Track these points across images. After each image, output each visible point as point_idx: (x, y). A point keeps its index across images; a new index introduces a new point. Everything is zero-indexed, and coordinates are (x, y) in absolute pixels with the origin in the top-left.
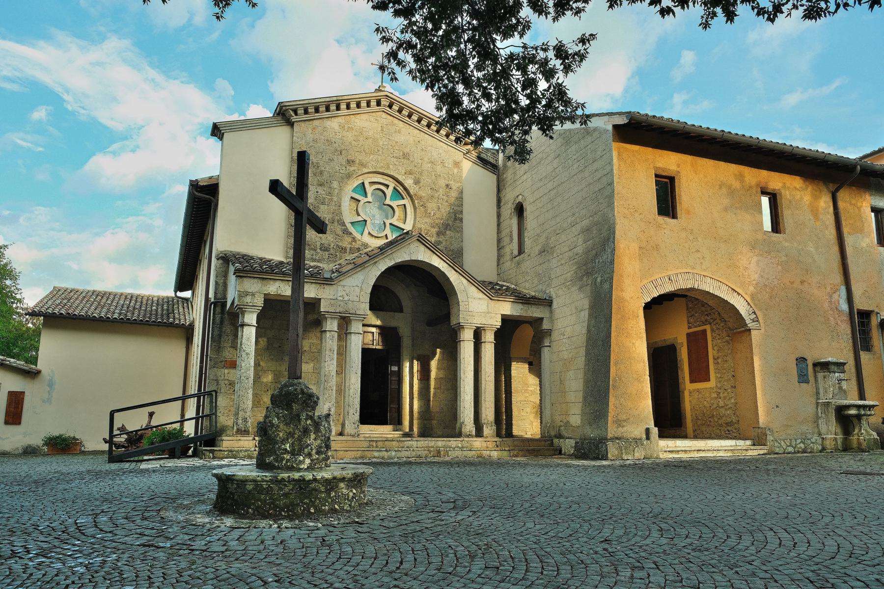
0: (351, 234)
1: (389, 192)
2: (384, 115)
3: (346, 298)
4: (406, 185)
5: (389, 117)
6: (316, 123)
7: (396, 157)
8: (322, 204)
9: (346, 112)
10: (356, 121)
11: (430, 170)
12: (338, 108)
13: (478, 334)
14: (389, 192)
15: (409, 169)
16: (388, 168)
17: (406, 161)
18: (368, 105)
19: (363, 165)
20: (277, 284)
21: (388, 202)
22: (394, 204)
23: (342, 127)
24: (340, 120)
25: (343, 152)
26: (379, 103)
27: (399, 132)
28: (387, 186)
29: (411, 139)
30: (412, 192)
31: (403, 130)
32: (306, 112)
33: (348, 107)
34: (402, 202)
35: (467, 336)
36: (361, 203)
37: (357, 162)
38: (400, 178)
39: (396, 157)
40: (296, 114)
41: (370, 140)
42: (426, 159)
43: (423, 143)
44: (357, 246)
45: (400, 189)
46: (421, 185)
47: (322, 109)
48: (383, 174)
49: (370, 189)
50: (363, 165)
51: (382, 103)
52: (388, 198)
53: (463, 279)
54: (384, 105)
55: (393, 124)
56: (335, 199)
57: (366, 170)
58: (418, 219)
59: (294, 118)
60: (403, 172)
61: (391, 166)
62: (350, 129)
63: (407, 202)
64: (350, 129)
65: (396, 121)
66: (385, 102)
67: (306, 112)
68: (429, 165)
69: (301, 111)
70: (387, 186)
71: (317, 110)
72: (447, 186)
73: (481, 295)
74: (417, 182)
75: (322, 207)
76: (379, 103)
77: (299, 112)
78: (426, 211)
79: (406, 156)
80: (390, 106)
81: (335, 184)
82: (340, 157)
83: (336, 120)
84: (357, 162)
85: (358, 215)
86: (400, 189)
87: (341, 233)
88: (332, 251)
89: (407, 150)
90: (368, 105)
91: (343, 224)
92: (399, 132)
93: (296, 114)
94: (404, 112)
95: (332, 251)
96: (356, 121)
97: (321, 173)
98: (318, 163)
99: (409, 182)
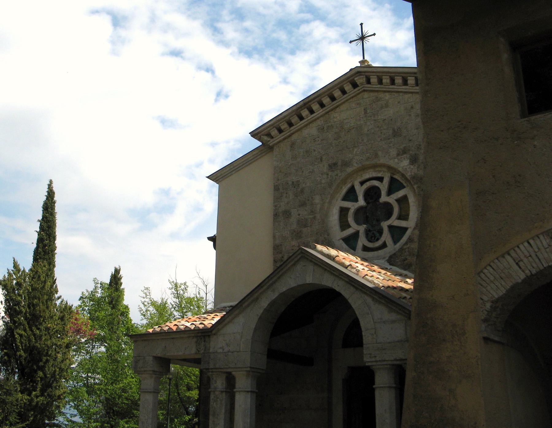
1: (384, 187)
2: (366, 95)
3: (226, 350)
5: (372, 94)
6: (294, 137)
8: (305, 226)
12: (312, 112)
13: (399, 372)
16: (376, 155)
21: (384, 198)
23: (321, 129)
24: (319, 122)
25: (324, 158)
26: (355, 85)
27: (387, 106)
28: (381, 179)
30: (408, 175)
32: (280, 131)
34: (400, 194)
35: (383, 380)
36: (351, 212)
37: (340, 163)
40: (272, 138)
45: (396, 177)
47: (295, 119)
49: (360, 191)
50: (346, 164)
52: (384, 193)
53: (366, 297)
54: (362, 84)
56: (318, 216)
57: (349, 170)
59: (271, 142)
61: (380, 153)
65: (381, 95)
67: (280, 131)
69: (274, 132)
70: (381, 179)
73: (394, 316)
74: (414, 160)
75: (305, 230)
76: (355, 85)
79: (396, 133)
80: (368, 81)
83: (314, 124)
84: (340, 163)
85: (349, 226)
93: (272, 138)
94: (384, 81)
97: (302, 191)
98: (298, 181)
99: (404, 164)
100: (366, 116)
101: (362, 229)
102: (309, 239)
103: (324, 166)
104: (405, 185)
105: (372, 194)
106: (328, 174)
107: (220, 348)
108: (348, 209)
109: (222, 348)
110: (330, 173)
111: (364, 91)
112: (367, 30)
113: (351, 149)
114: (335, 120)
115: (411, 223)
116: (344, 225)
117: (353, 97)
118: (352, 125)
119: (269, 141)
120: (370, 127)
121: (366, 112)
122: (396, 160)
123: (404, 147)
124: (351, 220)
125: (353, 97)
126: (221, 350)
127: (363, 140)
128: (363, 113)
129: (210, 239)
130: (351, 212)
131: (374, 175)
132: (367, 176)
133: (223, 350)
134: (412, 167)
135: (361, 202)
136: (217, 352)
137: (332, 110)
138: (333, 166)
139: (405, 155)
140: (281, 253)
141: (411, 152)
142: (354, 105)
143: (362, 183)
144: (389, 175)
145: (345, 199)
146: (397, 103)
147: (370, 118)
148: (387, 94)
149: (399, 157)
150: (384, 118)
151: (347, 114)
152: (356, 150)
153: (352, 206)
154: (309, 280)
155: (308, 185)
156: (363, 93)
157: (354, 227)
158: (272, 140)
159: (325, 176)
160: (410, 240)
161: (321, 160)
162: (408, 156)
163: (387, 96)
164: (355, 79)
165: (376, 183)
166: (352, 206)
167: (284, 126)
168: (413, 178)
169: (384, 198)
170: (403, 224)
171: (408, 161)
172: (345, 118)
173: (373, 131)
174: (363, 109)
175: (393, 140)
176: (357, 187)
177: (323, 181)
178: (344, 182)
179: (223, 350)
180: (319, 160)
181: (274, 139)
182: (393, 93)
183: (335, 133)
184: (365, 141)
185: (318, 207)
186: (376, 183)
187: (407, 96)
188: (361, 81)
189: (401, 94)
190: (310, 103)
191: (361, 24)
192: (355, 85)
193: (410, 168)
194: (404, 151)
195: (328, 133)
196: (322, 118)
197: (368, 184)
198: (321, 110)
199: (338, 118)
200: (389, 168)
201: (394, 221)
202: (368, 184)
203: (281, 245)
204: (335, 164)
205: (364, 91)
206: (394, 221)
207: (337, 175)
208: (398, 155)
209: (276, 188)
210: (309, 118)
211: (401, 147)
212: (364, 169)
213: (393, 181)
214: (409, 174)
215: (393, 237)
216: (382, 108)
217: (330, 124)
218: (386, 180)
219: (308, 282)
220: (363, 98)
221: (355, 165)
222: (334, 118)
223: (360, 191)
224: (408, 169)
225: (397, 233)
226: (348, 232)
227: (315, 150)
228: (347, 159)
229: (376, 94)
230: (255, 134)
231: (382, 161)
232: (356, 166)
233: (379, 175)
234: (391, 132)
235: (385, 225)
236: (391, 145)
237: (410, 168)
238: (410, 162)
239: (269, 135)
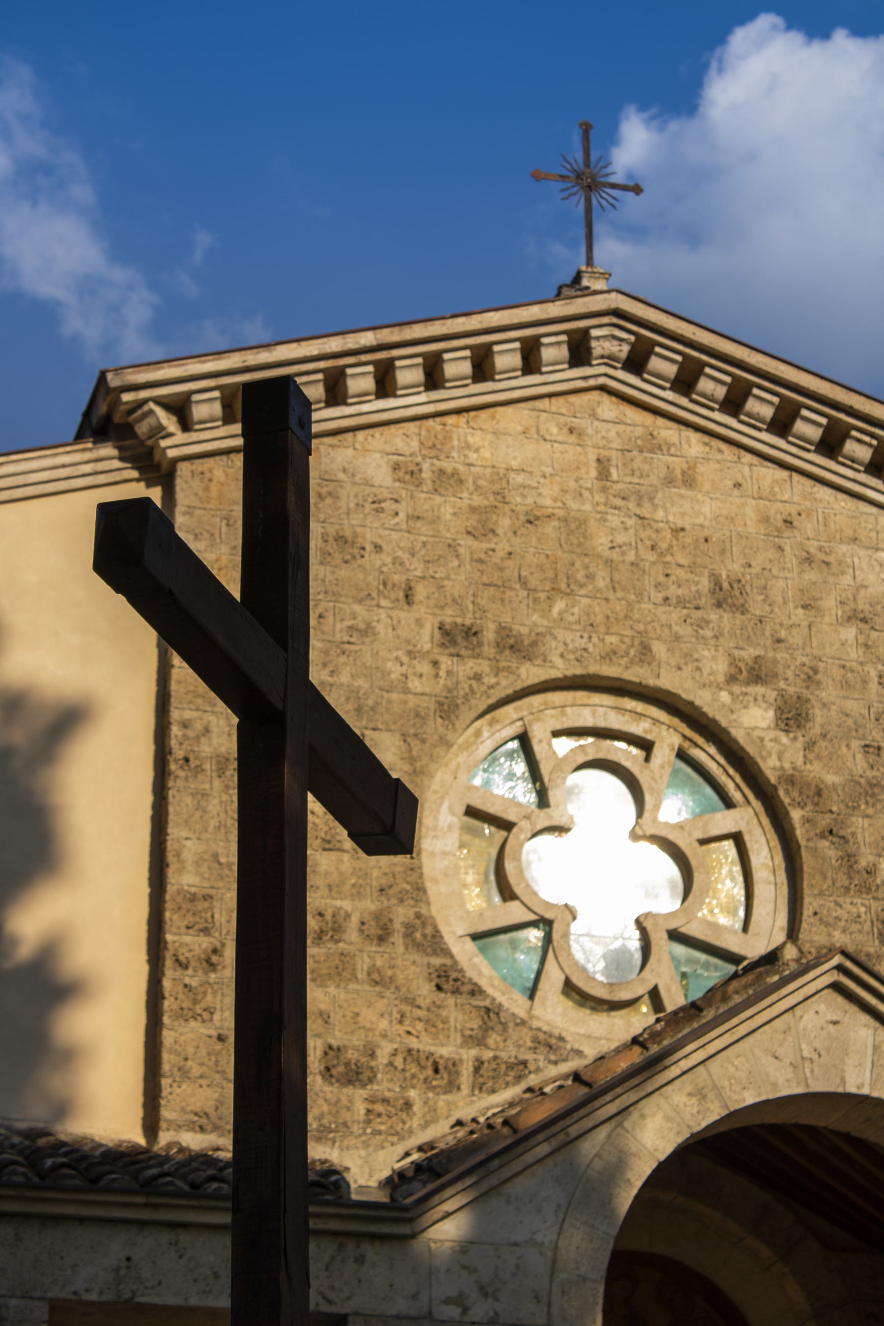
0: (476, 991)
2: (608, 408)
4: (738, 734)
7: (681, 602)
9: (421, 401)
10: (475, 439)
11: (854, 654)
12: (385, 385)
15: (749, 653)
16: (645, 653)
17: (725, 620)
18: (531, 361)
19: (515, 647)
20: (115, 1246)
23: (407, 472)
25: (421, 591)
27: (689, 480)
29: (750, 511)
30: (770, 767)
31: (706, 471)
33: (433, 378)
37: (490, 634)
38: (713, 703)
39: (681, 602)
40: (186, 425)
41: (550, 528)
42: (830, 603)
43: (808, 527)
44: (509, 1053)
46: (816, 730)
51: (598, 348)
54: (609, 359)
55: (653, 445)
58: (810, 904)
60: (722, 667)
61: (659, 649)
62: (447, 480)
63: (747, 818)
64: (447, 480)
65: (668, 432)
66: (607, 343)
68: (850, 633)
74: (792, 716)
76: (579, 352)
77: (199, 412)
78: (849, 859)
79: (726, 595)
80: (636, 363)
82: (405, 616)
83: (377, 439)
84: (490, 634)
86: (708, 755)
87: (425, 990)
88: (384, 1086)
89: (731, 567)
90: (531, 361)
91: (435, 943)
92: (689, 480)
94: (704, 385)
95: (385, 1085)
96: (475, 439)
99: (751, 720)
100: (604, 490)
102: (346, 905)
103: (419, 622)
104: (736, 796)
106: (435, 663)
107: (448, 1301)
109: (459, 1300)
110: (446, 663)
111: (603, 388)
113: (542, 596)
114: (473, 457)
117: (550, 395)
118: (548, 502)
119: (170, 435)
120: (621, 538)
121: (604, 474)
122: (724, 696)
123: (757, 658)
125: (550, 395)
126: (453, 1312)
127: (590, 577)
128: (593, 473)
131: (615, 722)
133: (465, 1310)
134: (784, 739)
136: (430, 1315)
137: (458, 412)
138: (457, 637)
139: (759, 689)
140: (206, 931)
141: (782, 684)
142: (554, 430)
144: (676, 740)
146: (730, 484)
147: (618, 502)
148: (695, 437)
149: (737, 689)
150: (680, 524)
152: (559, 605)
155: (344, 678)
156: (595, 395)
158: (180, 437)
159: (425, 668)
161: (408, 598)
162: (772, 695)
163: (694, 445)
164: (594, 333)
168: (791, 780)
171: (771, 714)
172: (514, 464)
173: (631, 556)
174: (592, 457)
175: (713, 616)
177: (415, 684)
179: (465, 1310)
180: (401, 595)
181: (194, 436)
182: (716, 443)
183: (473, 509)
184: (601, 583)
187: (772, 473)
188: (611, 347)
189: (748, 457)
190: (395, 353)
192: (579, 352)
193: (775, 740)
194: (757, 674)
195: (438, 499)
196: (411, 427)
198: (423, 398)
199: (486, 453)
203: (207, 897)
204: (471, 633)
205: (603, 388)
207: (478, 677)
208: (732, 679)
210: (365, 408)
211: (744, 654)
214: (773, 762)
216: (669, 481)
217: (448, 466)
219: (852, 1089)
220: (594, 415)
221: (558, 662)
222: (468, 446)
224: (769, 745)
227: (378, 548)
228: (524, 630)
229: (647, 418)
231: (666, 681)
232: (560, 669)
233: (638, 728)
234: (705, 583)
236: (708, 633)
237: (775, 740)
238: (778, 719)
239: (180, 409)
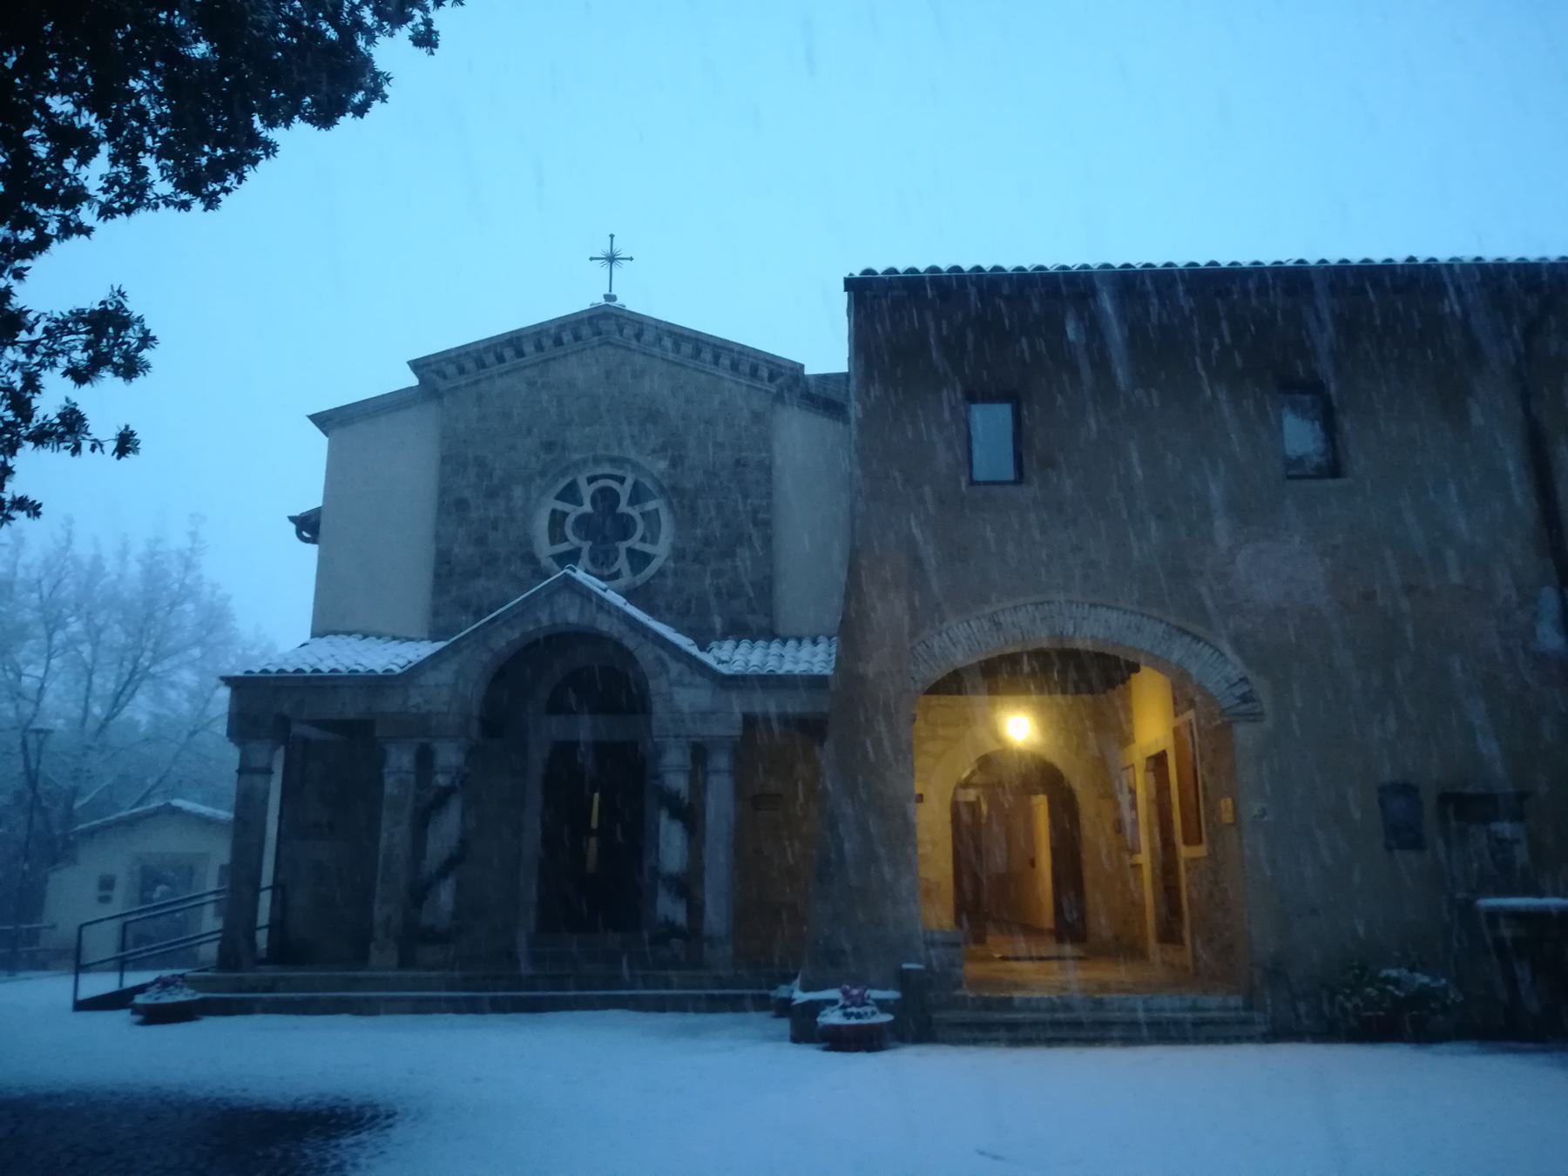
1: (624, 491)
13: (699, 753)
14: (624, 491)
21: (623, 507)
22: (634, 512)
28: (622, 480)
36: (570, 520)
40: (445, 377)
48: (613, 461)
49: (587, 491)
52: (624, 500)
59: (443, 385)
71: (481, 364)
72: (738, 462)
81: (518, 492)
85: (566, 540)
101: (586, 546)
105: (606, 498)
108: (565, 515)
112: (622, 248)
115: (661, 550)
116: (556, 534)
124: (569, 531)
129: (292, 519)
130: (570, 520)
132: (599, 471)
135: (587, 507)
143: (591, 480)
145: (561, 497)
151: (580, 371)
153: (573, 511)
154: (573, 617)
157: (574, 541)
160: (661, 573)
165: (614, 484)
166: (573, 511)
167: (470, 365)
169: (623, 507)
170: (647, 548)
176: (582, 482)
178: (563, 474)
185: (519, 503)
186: (614, 484)
191: (612, 236)
197: (602, 483)
200: (636, 467)
201: (635, 542)
202: (602, 483)
206: (635, 542)
209: (444, 460)
212: (597, 461)
213: (636, 484)
215: (631, 563)
218: (629, 482)
223: (587, 491)
225: (639, 560)
226: (563, 547)
230: (416, 365)
233: (619, 473)
235: (623, 546)
